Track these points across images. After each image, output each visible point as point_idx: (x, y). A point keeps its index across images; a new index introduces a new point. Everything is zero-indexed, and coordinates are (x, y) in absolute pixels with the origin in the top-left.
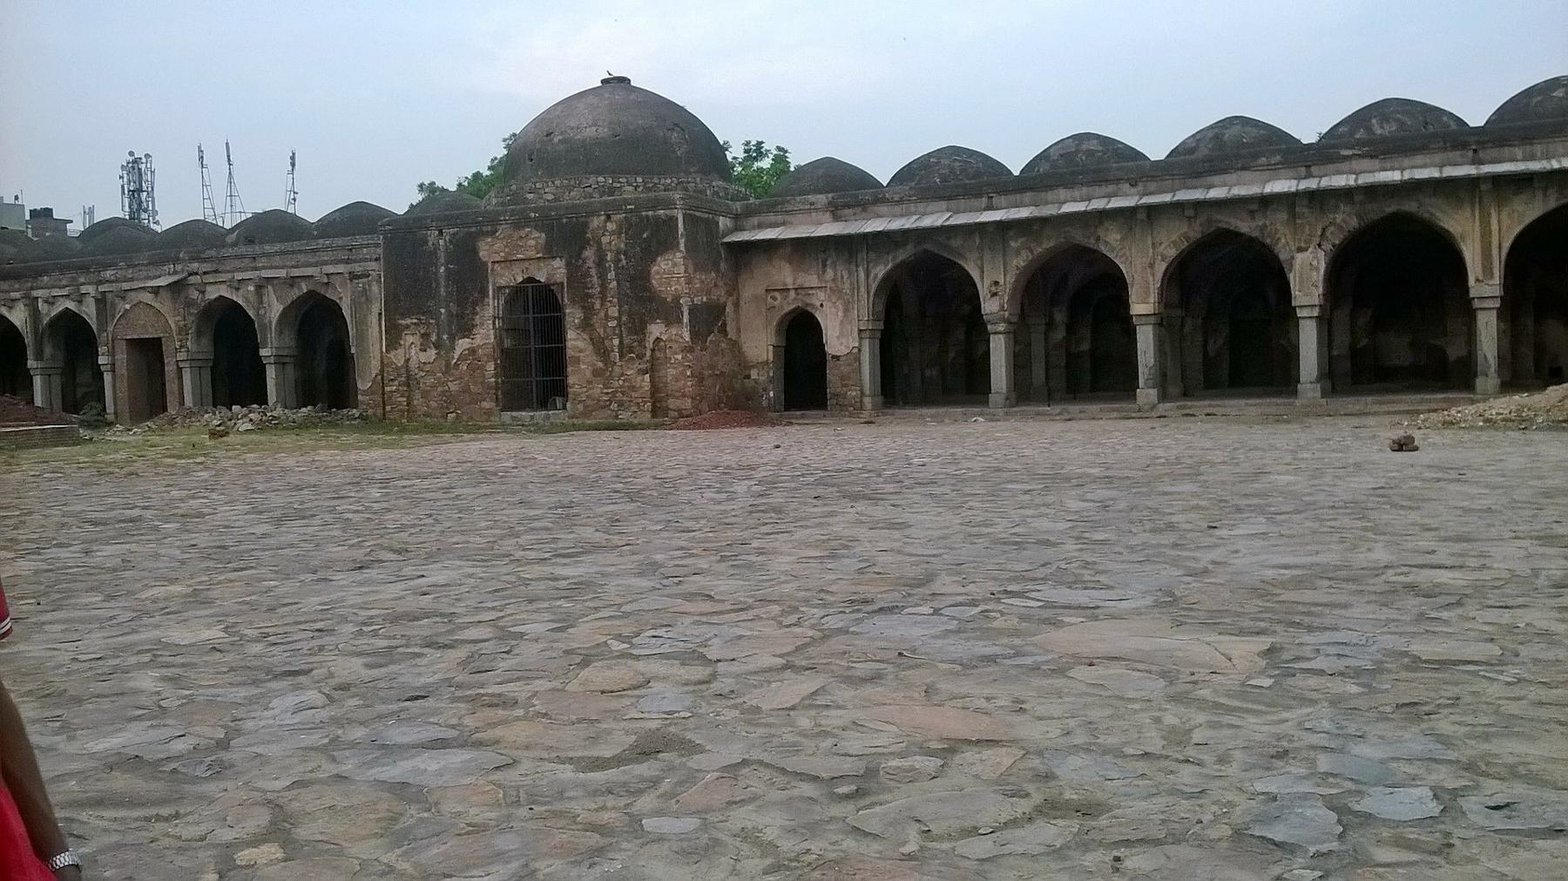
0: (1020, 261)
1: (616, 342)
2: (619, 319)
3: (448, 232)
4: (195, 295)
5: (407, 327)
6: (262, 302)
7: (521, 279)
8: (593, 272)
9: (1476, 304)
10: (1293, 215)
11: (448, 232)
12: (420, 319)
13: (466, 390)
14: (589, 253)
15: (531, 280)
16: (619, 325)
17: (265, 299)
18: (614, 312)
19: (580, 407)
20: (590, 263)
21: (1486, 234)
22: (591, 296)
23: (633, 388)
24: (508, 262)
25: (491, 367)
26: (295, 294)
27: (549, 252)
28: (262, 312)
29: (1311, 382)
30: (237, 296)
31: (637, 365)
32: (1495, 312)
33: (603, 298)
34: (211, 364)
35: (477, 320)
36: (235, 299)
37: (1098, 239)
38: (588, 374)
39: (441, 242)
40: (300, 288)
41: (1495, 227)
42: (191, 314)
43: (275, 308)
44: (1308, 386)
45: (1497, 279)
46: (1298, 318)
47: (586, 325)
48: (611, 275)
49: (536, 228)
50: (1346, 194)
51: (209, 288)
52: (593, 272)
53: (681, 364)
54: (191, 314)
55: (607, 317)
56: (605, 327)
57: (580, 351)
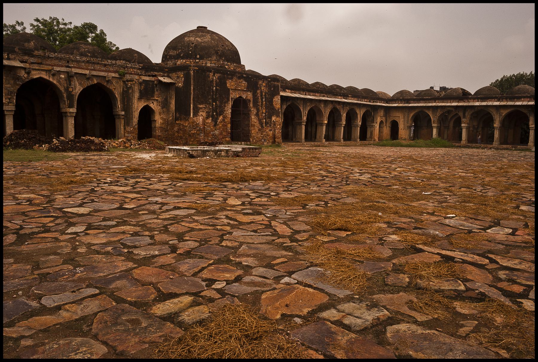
1: (264, 121)
2: (265, 113)
3: (217, 75)
4: (23, 74)
5: (201, 108)
6: (70, 85)
7: (238, 96)
8: (260, 98)
9: (6, 113)
11: (217, 75)
12: (206, 106)
13: (221, 134)
14: (259, 91)
15: (240, 97)
16: (265, 116)
17: (73, 83)
18: (264, 111)
19: (254, 141)
20: (259, 95)
22: (259, 105)
23: (268, 135)
24: (235, 90)
25: (229, 126)
26: (90, 83)
27: (249, 89)
28: (71, 90)
30: (54, 79)
31: (269, 129)
33: (262, 107)
34: (74, 115)
35: (226, 109)
36: (51, 80)
38: (257, 130)
39: (214, 78)
40: (92, 80)
42: (18, 85)
43: (78, 89)
47: (257, 115)
48: (264, 100)
49: (246, 81)
51: (33, 72)
52: (260, 98)
53: (279, 129)
54: (18, 85)
55: (262, 113)
56: (262, 116)
57: (255, 123)
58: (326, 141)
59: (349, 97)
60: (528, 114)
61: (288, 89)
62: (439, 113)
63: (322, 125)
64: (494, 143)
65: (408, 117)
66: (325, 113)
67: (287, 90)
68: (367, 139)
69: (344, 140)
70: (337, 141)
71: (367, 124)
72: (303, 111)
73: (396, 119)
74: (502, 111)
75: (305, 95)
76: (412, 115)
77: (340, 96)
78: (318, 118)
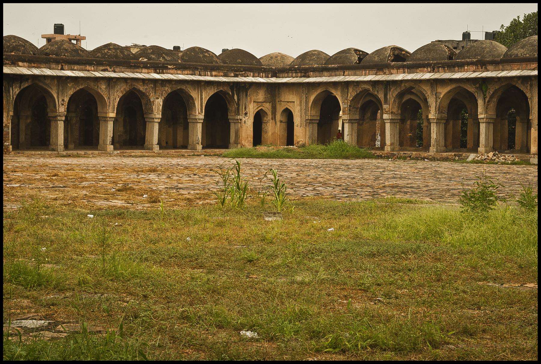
0: (71, 92)
10: (155, 86)
21: (201, 99)
29: (156, 145)
32: (201, 124)
37: (98, 87)
41: (203, 97)
44: (156, 146)
45: (203, 114)
46: (189, 122)
50: (170, 81)
58: (115, 149)
59: (167, 68)
60: (476, 96)
61: (23, 61)
62: (352, 93)
63: (106, 120)
64: (431, 148)
65: (307, 103)
66: (109, 98)
67: (20, 64)
68: (231, 145)
69: (161, 148)
70: (149, 149)
71: (229, 117)
72: (58, 97)
73: (290, 107)
74: (439, 90)
75: (62, 69)
76: (312, 98)
77: (146, 67)
78: (99, 109)
